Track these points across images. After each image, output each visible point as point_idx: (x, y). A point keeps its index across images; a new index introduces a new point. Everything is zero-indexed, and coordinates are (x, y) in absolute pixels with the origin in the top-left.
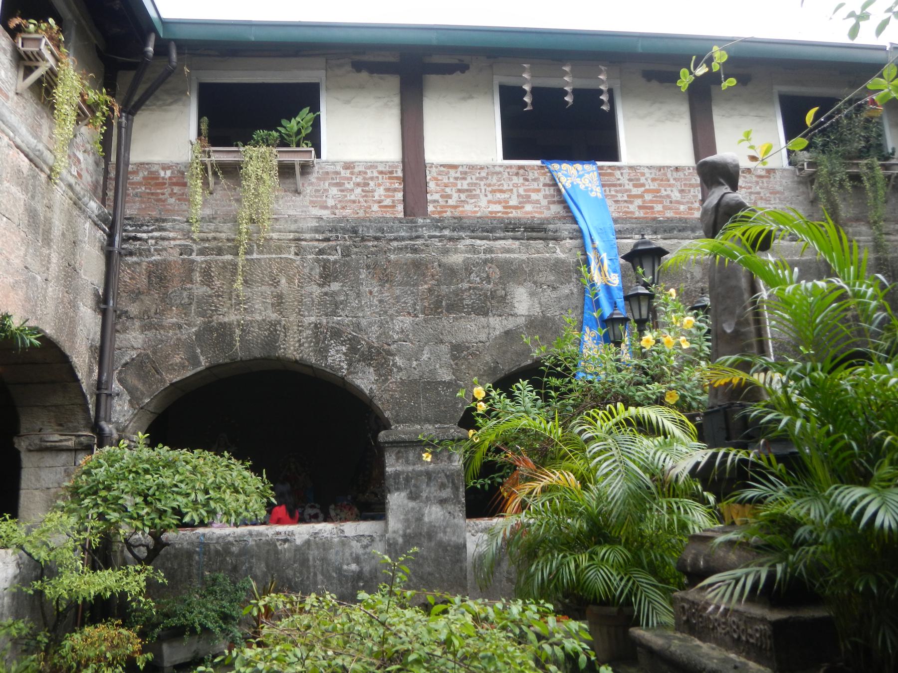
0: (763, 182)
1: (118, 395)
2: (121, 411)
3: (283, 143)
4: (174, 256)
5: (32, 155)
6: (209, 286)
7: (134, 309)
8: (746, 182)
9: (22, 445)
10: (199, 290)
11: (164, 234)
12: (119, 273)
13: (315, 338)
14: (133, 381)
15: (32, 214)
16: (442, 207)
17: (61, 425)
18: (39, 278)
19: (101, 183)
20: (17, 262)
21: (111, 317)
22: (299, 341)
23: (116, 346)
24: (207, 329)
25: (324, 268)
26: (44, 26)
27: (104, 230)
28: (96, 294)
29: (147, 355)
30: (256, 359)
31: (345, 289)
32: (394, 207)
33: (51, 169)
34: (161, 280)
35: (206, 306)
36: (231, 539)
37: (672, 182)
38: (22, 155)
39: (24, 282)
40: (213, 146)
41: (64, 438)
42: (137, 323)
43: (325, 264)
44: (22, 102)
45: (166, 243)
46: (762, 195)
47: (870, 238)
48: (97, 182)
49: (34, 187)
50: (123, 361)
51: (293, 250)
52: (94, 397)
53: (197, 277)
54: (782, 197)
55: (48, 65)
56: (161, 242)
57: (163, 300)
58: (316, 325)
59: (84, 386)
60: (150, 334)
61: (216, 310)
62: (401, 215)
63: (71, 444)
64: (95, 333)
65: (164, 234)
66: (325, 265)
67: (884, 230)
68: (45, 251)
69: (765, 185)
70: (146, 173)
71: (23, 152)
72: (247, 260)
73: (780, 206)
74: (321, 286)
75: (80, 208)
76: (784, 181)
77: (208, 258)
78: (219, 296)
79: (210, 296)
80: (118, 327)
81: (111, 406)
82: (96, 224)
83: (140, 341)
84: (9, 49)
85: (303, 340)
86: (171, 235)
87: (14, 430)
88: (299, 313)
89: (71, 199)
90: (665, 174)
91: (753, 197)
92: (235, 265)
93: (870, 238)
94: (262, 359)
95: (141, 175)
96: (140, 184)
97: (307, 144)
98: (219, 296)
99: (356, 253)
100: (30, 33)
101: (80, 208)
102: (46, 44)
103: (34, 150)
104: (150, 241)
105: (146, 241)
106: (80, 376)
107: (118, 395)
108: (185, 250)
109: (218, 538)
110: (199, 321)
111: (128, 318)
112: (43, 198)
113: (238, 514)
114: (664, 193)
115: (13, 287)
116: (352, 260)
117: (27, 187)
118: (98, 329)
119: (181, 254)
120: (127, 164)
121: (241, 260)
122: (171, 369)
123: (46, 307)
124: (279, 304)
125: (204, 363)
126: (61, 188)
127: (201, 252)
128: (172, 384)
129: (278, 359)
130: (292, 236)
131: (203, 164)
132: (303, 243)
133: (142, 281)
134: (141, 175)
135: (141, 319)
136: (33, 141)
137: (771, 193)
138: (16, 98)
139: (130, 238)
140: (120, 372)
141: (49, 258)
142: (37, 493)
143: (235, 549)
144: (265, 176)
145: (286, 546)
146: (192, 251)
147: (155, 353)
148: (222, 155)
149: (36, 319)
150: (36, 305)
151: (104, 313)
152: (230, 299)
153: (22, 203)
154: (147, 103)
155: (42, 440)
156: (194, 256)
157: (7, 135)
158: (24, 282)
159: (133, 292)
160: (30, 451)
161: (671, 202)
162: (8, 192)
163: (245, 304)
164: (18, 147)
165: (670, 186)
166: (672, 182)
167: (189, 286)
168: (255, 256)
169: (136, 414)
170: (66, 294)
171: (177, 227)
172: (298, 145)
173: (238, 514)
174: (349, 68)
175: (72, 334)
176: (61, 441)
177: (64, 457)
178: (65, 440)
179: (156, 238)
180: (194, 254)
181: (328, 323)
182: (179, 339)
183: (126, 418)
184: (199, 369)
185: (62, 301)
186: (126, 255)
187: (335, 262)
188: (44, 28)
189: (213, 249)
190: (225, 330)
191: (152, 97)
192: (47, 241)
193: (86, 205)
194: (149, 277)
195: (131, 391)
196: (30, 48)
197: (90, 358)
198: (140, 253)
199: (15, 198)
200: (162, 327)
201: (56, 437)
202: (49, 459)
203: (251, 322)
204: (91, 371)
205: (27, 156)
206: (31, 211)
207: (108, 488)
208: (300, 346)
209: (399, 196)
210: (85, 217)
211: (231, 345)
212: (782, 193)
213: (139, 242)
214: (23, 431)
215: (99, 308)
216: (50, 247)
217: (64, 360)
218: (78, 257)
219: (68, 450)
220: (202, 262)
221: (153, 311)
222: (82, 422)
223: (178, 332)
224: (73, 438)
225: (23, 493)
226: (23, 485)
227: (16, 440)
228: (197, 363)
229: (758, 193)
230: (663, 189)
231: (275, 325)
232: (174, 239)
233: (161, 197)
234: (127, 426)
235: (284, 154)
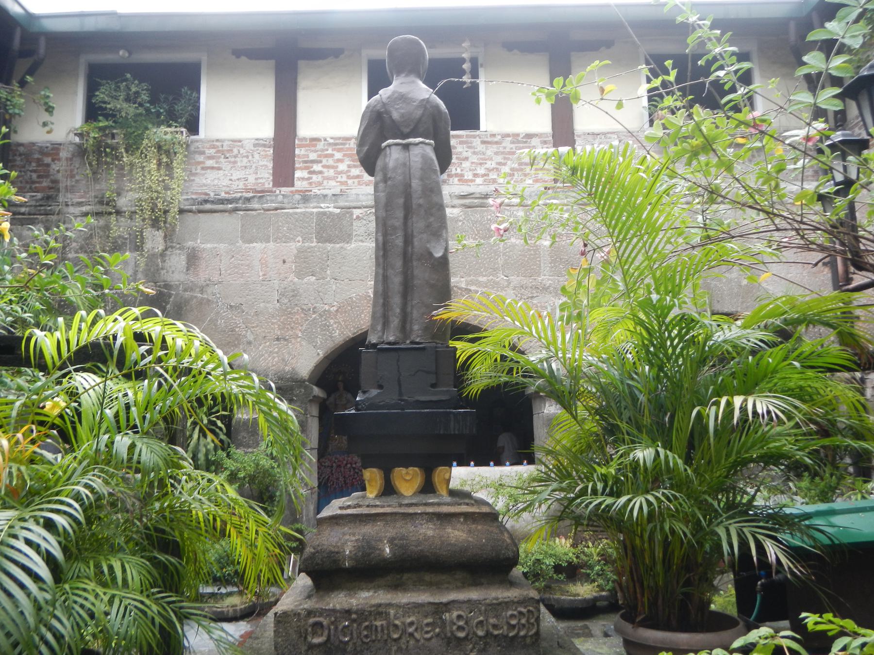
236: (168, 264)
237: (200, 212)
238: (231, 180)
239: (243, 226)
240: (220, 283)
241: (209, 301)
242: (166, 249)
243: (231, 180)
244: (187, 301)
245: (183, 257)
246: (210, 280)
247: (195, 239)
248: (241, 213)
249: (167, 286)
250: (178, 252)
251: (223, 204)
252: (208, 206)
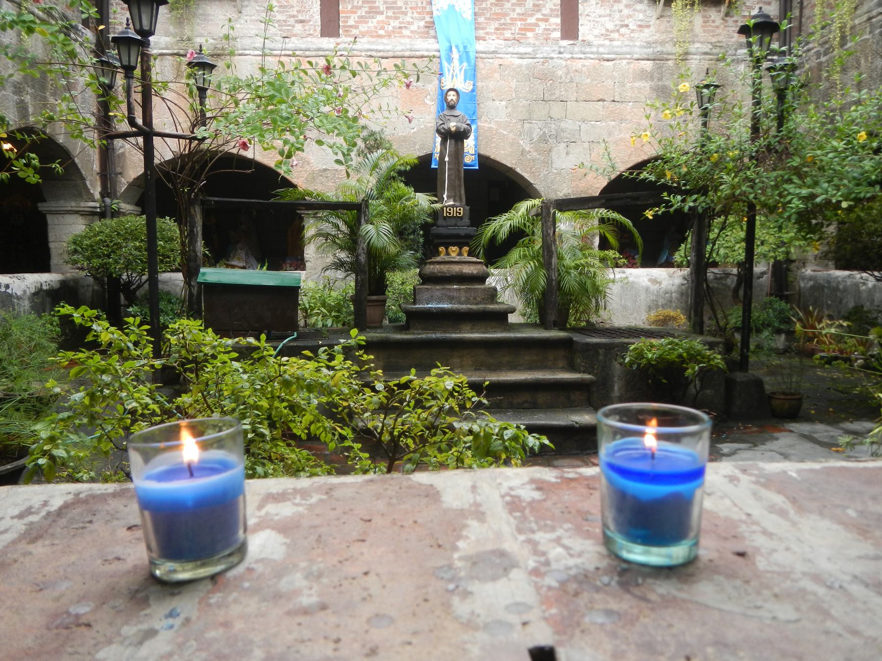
5: (652, 57)
36: (840, 279)
44: (665, 19)
51: (868, 29)
71: (643, 60)
86: (811, 46)
103: (653, 53)
108: (818, 55)
112: (672, 74)
127: (825, 54)
130: (865, 18)
132: (874, 20)
138: (658, 22)
143: (841, 287)
145: (864, 288)
157: (626, 59)
164: (638, 60)
205: (648, 60)
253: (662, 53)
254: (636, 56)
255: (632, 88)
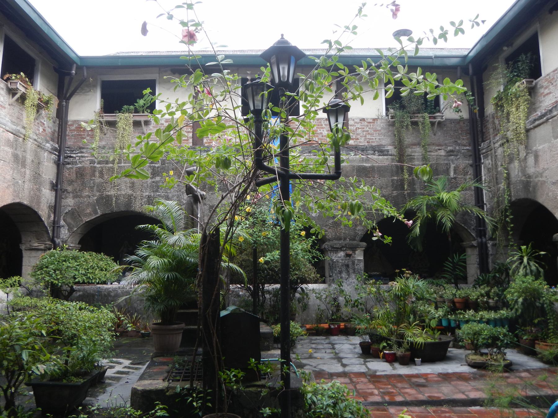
0: (370, 125)
1: (63, 226)
2: (64, 233)
3: (136, 111)
4: (87, 165)
5: (14, 132)
6: (102, 178)
7: (70, 189)
8: (362, 126)
9: (23, 247)
10: (98, 180)
11: (83, 155)
12: (63, 172)
13: (148, 202)
14: (69, 220)
15: (16, 157)
16: (210, 140)
17: (38, 239)
18: (20, 182)
19: (57, 130)
20: (8, 177)
21: (59, 192)
22: (141, 203)
23: (62, 205)
24: (101, 198)
25: (153, 170)
26: (18, 77)
27: (55, 154)
28: (52, 183)
29: (75, 209)
30: (122, 211)
31: (162, 180)
32: (188, 140)
33: (25, 136)
34: (82, 175)
35: (101, 187)
36: (111, 290)
37: (324, 126)
38: (10, 134)
39: (13, 185)
40: (105, 113)
41: (39, 245)
42: (71, 195)
43: (153, 168)
44: (12, 107)
45: (84, 159)
46: (369, 132)
47: (420, 154)
48: (55, 130)
49: (16, 145)
50: (65, 212)
52: (52, 228)
53: (97, 174)
54: (380, 133)
55: (22, 92)
56: (81, 158)
57: (82, 185)
58: (149, 196)
59: (46, 223)
60: (77, 200)
61: (105, 189)
62: (191, 145)
63: (42, 247)
64: (52, 200)
65: (83, 155)
66: (154, 169)
67: (428, 150)
68: (23, 170)
69: (372, 126)
70: (77, 125)
71: (10, 132)
72: (119, 166)
73: (379, 137)
74: (151, 178)
75: (41, 148)
76: (382, 124)
77: (102, 165)
78: (106, 183)
79: (103, 183)
80: (63, 197)
81: (60, 231)
82: (50, 152)
83: (72, 203)
84: (5, 87)
85: (143, 203)
86: (86, 155)
87: (19, 241)
88: (141, 191)
89: (36, 145)
90: (321, 122)
91: (364, 133)
92: (113, 168)
93: (420, 154)
94: (124, 211)
95: (75, 126)
96: (74, 130)
97: (147, 111)
98: (106, 183)
99: (168, 163)
100: (13, 80)
101: (41, 148)
102: (20, 84)
103: (15, 130)
104: (77, 158)
105: (75, 158)
106: (43, 219)
107: (63, 226)
108: (92, 162)
109: (106, 289)
110: (98, 194)
111: (68, 192)
112: (21, 148)
113: (100, 279)
114: (319, 132)
115: (7, 188)
116: (166, 166)
117: (12, 146)
118: (53, 198)
119: (90, 164)
120: (66, 122)
121: (116, 166)
122: (86, 215)
123: (24, 193)
124: (133, 187)
125: (100, 213)
126: (31, 142)
127: (99, 163)
128: (86, 222)
129: (132, 211)
131: (100, 122)
133: (74, 176)
134: (75, 126)
135: (73, 193)
136: (14, 127)
137: (374, 131)
139: (68, 157)
140: (64, 217)
141: (25, 173)
142: (29, 267)
143: (112, 294)
144: (127, 128)
146: (95, 162)
147: (78, 208)
148: (109, 117)
149: (19, 199)
150: (19, 193)
151: (56, 191)
152: (111, 184)
153: (10, 153)
154: (78, 91)
155: (31, 246)
156: (96, 165)
157: (2, 128)
158: (13, 185)
159: (69, 181)
160: (26, 250)
161: (322, 136)
162: (3, 150)
163: (117, 187)
165: (322, 128)
166: (324, 126)
167: (93, 178)
168: (122, 165)
169: (71, 235)
170: (34, 186)
171: (88, 151)
172: (143, 112)
173: (100, 279)
174: (170, 72)
175: (38, 203)
176: (38, 246)
177: (40, 252)
178: (40, 246)
179: (79, 157)
180: (96, 164)
181: (154, 195)
182: (89, 202)
183: (66, 236)
184: (98, 216)
185: (33, 189)
186: (66, 164)
187: (158, 167)
188: (18, 77)
189: (104, 161)
190: (108, 199)
191: (80, 89)
192: (24, 165)
193: (44, 146)
194: (76, 174)
195: (68, 225)
196: (14, 87)
197: (48, 211)
198: (72, 163)
199: (7, 152)
200: (82, 197)
201: (36, 244)
202: (34, 254)
203: (120, 194)
204: (49, 217)
205: (12, 133)
206: (15, 155)
207: (47, 267)
208: (141, 206)
209: (191, 135)
210: (45, 151)
211: (111, 205)
212: (380, 131)
213: (72, 159)
214: (23, 242)
215: (53, 189)
216: (25, 167)
217: (36, 213)
218: (41, 169)
219: (41, 250)
220: (99, 167)
221: (78, 189)
222: (47, 238)
223: (88, 199)
224: (43, 245)
225: (23, 267)
226: (24, 264)
227: (20, 245)
228: (97, 213)
229: (368, 131)
230: (319, 130)
231: (131, 196)
232: (87, 157)
233: (83, 136)
234: (67, 240)
235: (136, 117)
236: (527, 164)
237: (535, 127)
238: (556, 98)
239: (553, 128)
240: (548, 169)
241: (545, 181)
242: (527, 155)
243: (556, 98)
244: (537, 184)
245: (533, 158)
246: (544, 169)
247: (536, 145)
248: (550, 120)
249: (529, 177)
250: (531, 155)
251: (542, 118)
252: (537, 123)
253: (19, 131)
254: (7, 128)
255: (3, 150)
